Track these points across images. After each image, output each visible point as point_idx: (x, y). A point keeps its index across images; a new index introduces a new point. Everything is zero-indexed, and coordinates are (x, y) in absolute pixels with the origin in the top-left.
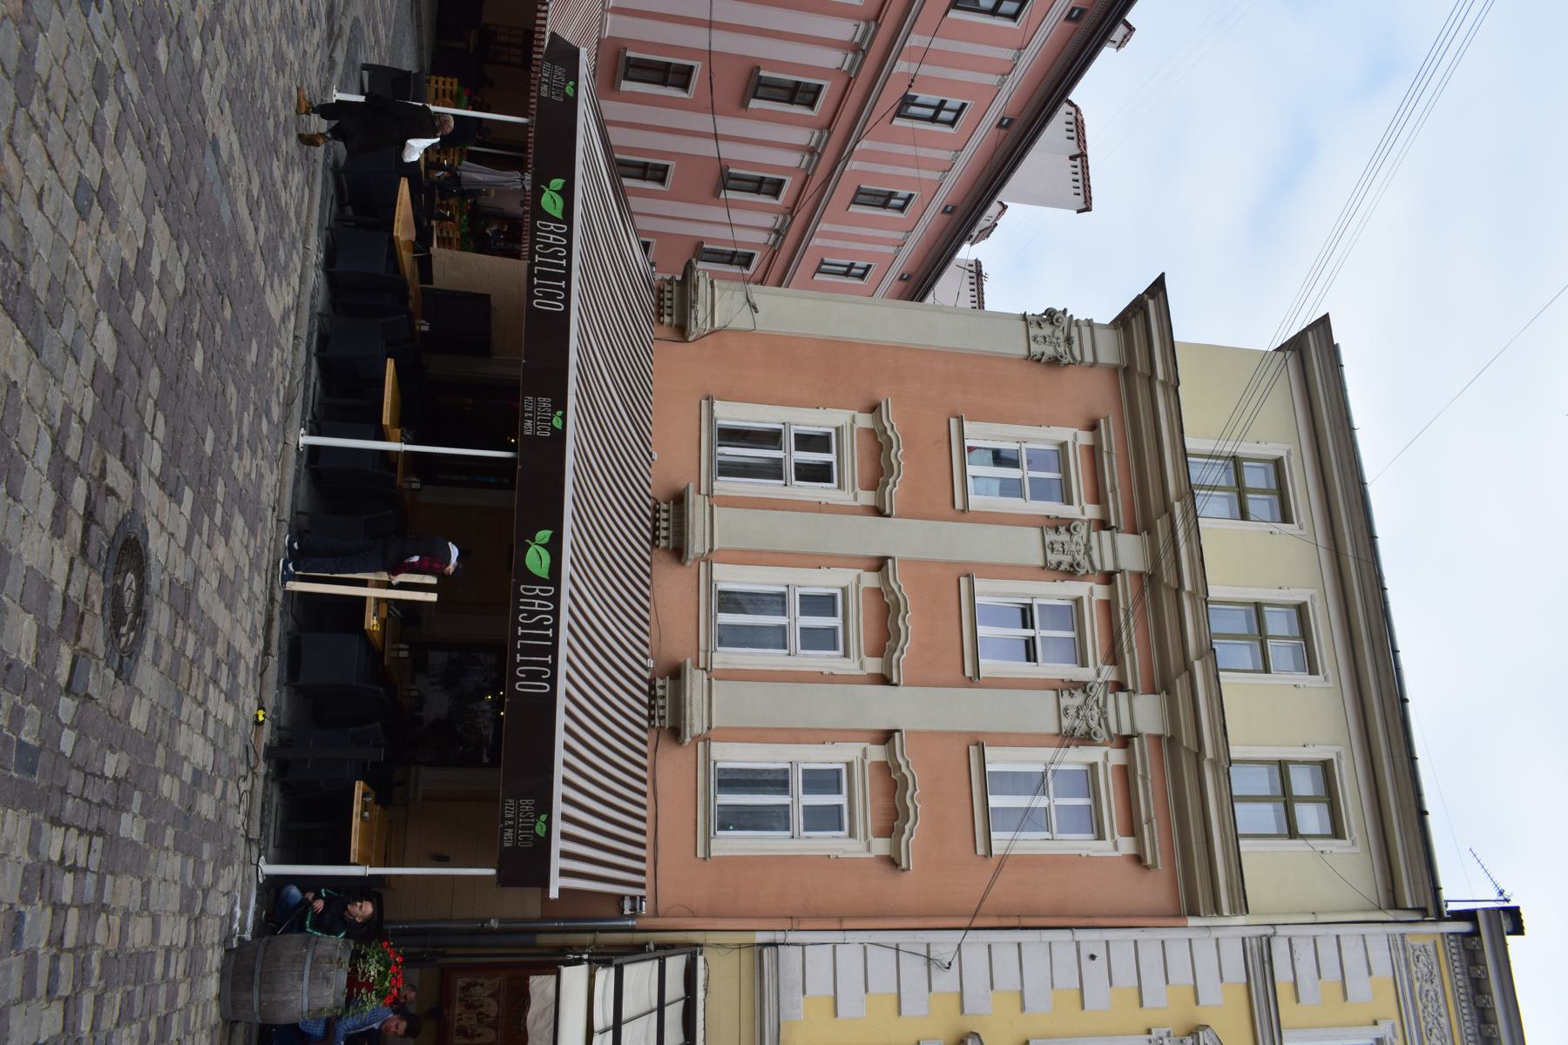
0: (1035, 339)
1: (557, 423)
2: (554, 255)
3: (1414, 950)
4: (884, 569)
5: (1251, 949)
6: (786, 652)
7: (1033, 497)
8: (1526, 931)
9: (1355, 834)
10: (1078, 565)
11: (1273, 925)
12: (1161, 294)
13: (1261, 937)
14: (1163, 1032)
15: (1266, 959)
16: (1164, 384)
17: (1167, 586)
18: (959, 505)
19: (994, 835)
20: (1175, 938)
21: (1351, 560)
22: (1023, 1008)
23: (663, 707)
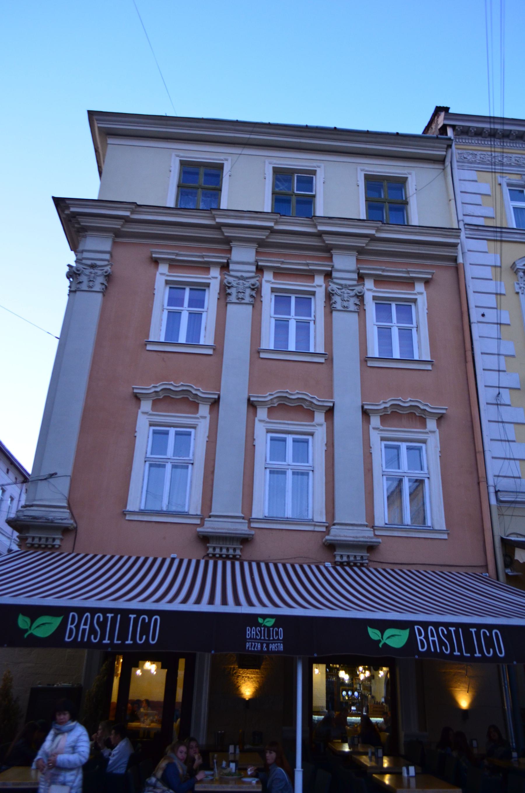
0: (90, 287)
1: (270, 622)
2: (102, 625)
3: (461, 159)
4: (256, 404)
5: (470, 234)
6: (311, 473)
7: (203, 307)
8: (448, 106)
9: (406, 172)
10: (253, 285)
11: (458, 221)
12: (67, 202)
13: (465, 228)
14: (517, 286)
15: (476, 228)
16: (133, 212)
17: (267, 237)
18: (210, 352)
19: (416, 358)
20: (470, 272)
21: (252, 136)
22: (513, 356)
23: (355, 557)
